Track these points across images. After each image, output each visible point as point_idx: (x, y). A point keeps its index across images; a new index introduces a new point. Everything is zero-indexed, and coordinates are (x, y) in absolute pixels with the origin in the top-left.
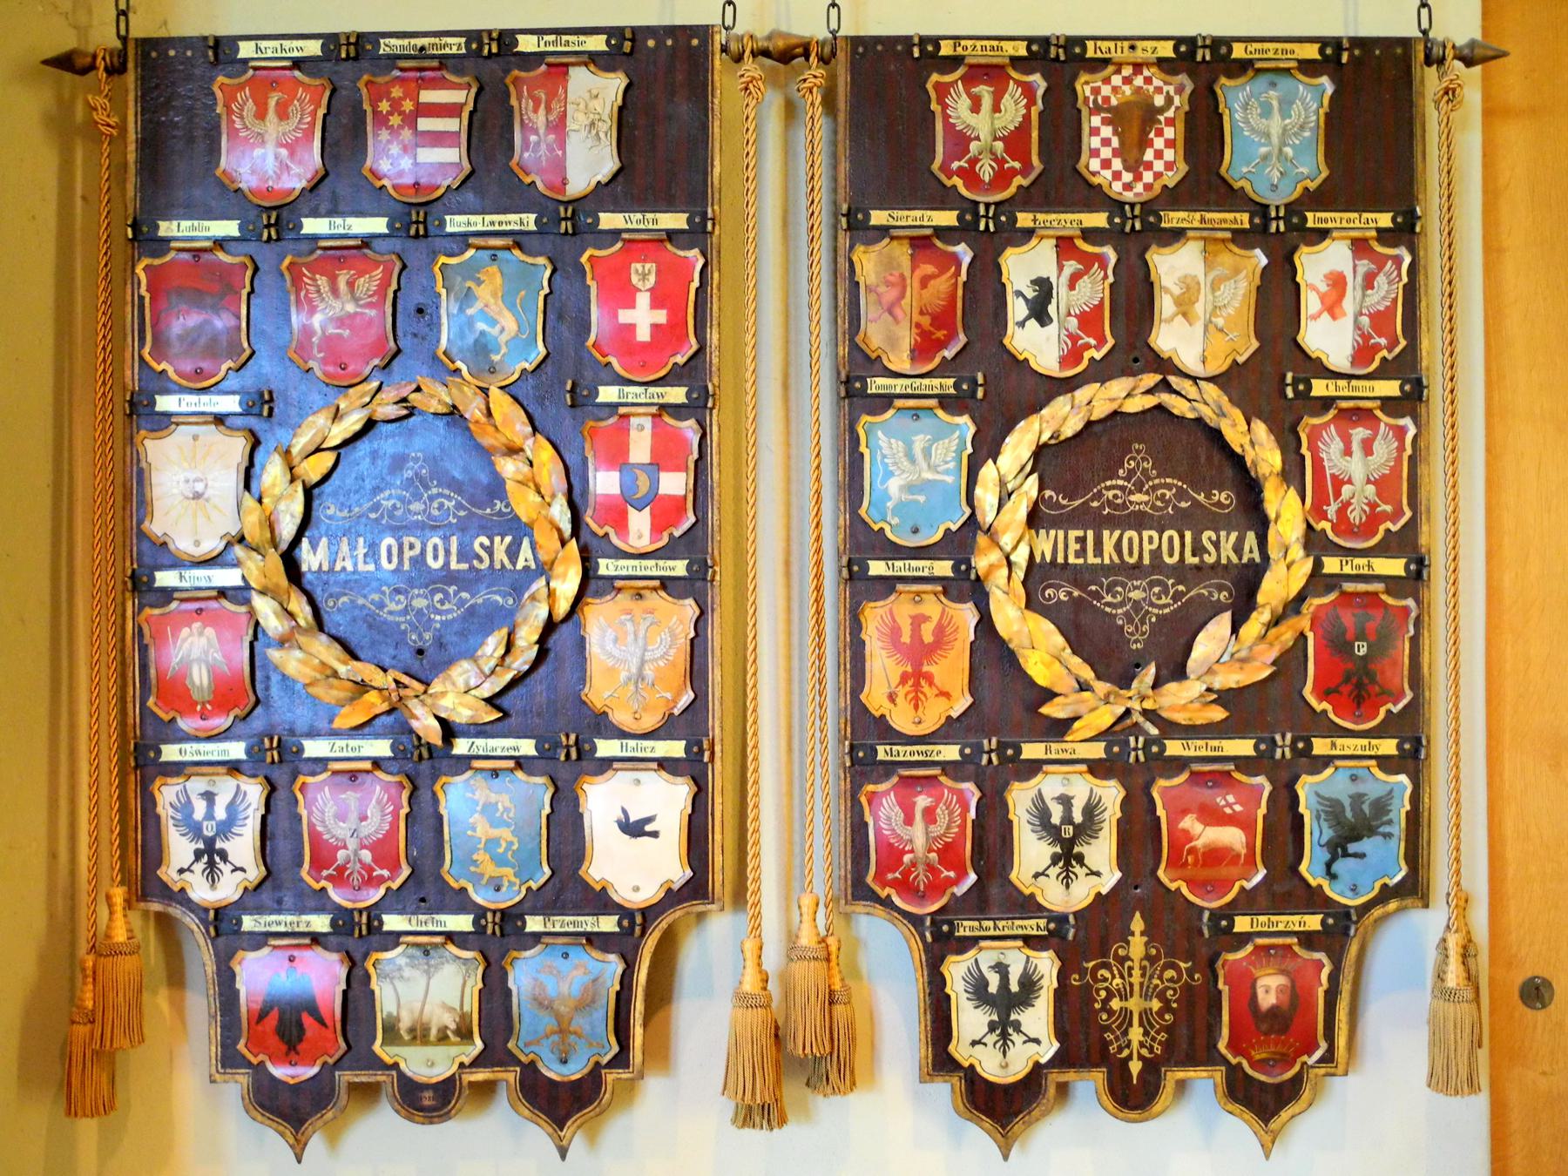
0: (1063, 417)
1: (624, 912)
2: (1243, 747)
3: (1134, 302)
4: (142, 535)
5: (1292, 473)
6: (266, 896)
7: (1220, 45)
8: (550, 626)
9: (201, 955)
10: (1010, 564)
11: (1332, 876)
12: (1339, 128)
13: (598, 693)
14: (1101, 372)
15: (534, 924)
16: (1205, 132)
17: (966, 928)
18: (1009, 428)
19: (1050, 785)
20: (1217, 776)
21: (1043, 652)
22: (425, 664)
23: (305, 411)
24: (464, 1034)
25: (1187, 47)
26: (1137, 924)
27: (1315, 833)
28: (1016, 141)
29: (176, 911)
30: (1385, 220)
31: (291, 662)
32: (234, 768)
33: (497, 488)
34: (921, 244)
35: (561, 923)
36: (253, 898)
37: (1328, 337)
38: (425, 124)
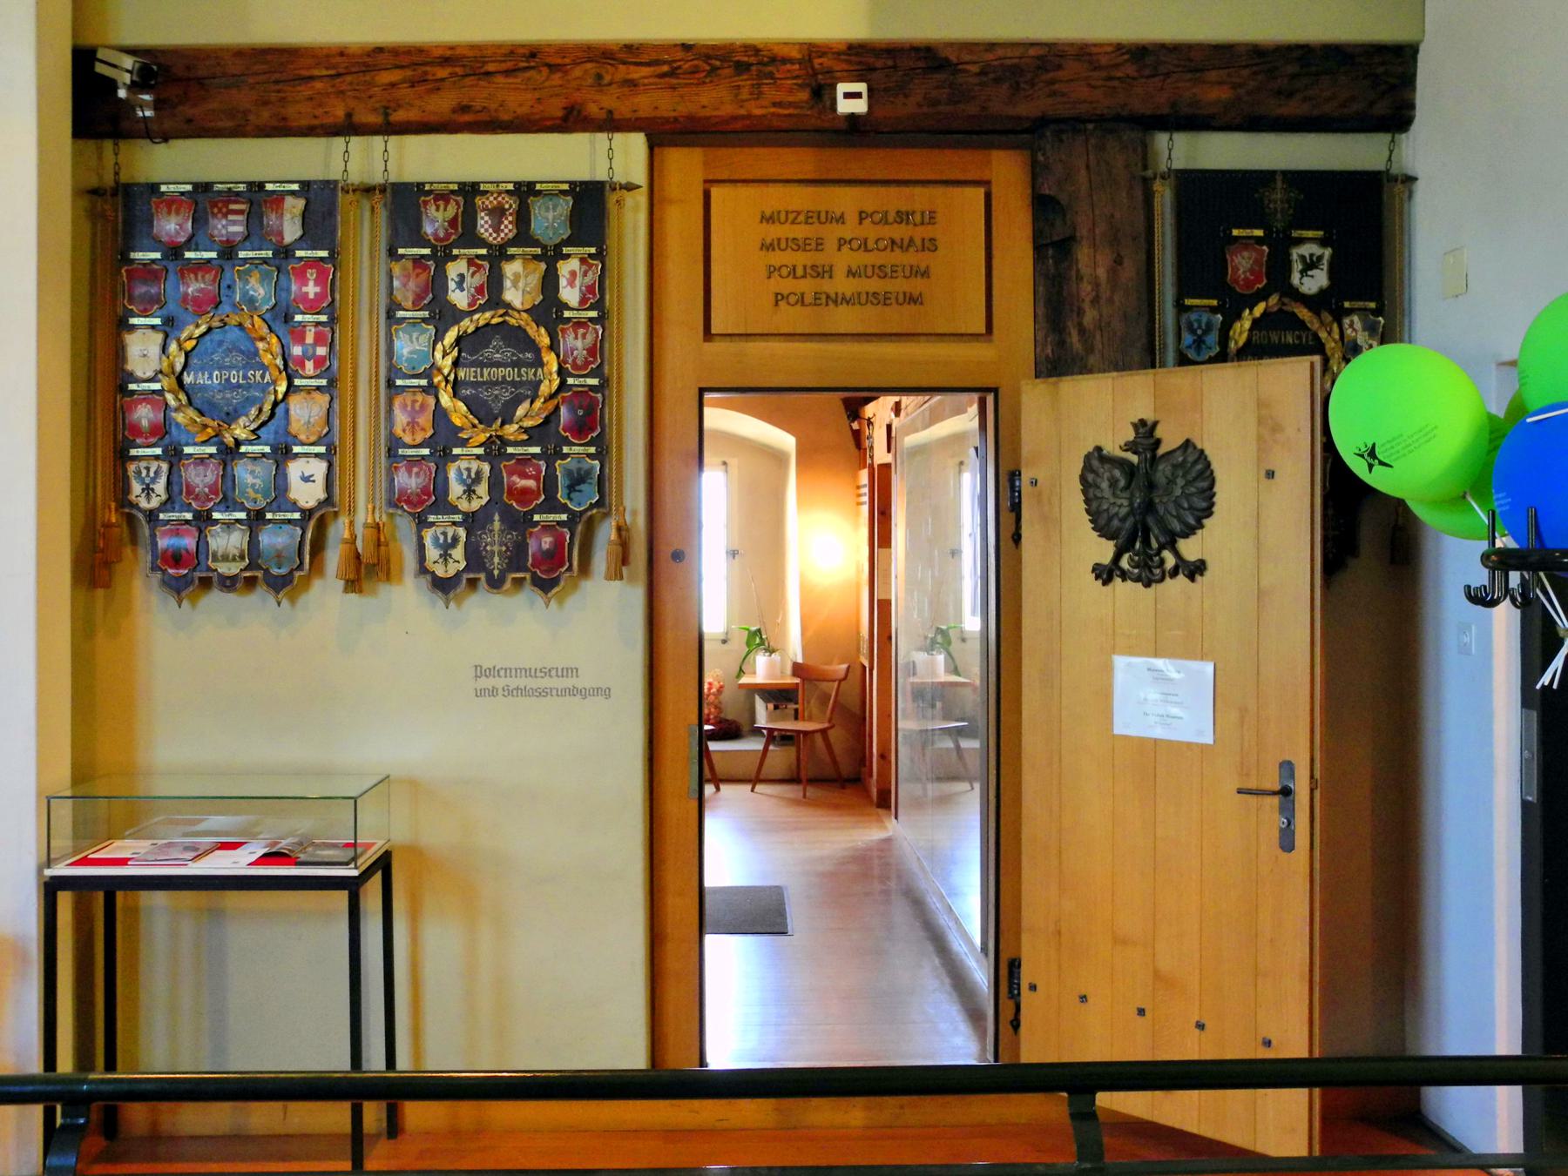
0: (468, 325)
1: (303, 511)
2: (536, 450)
3: (495, 283)
4: (123, 370)
5: (553, 347)
6: (169, 506)
7: (531, 185)
8: (276, 404)
9: (145, 530)
10: (447, 381)
11: (570, 499)
12: (575, 218)
13: (295, 427)
14: (482, 309)
15: (269, 516)
16: (523, 218)
17: (432, 518)
18: (446, 331)
19: (463, 464)
20: (525, 460)
21: (459, 413)
22: (230, 418)
23: (185, 324)
24: (242, 557)
25: (518, 184)
26: (497, 517)
27: (562, 481)
28: (453, 223)
29: (134, 512)
30: (593, 250)
31: (180, 417)
32: (157, 457)
33: (256, 353)
34: (418, 261)
35: (280, 516)
36: (164, 507)
37: (569, 294)
38: (231, 217)
